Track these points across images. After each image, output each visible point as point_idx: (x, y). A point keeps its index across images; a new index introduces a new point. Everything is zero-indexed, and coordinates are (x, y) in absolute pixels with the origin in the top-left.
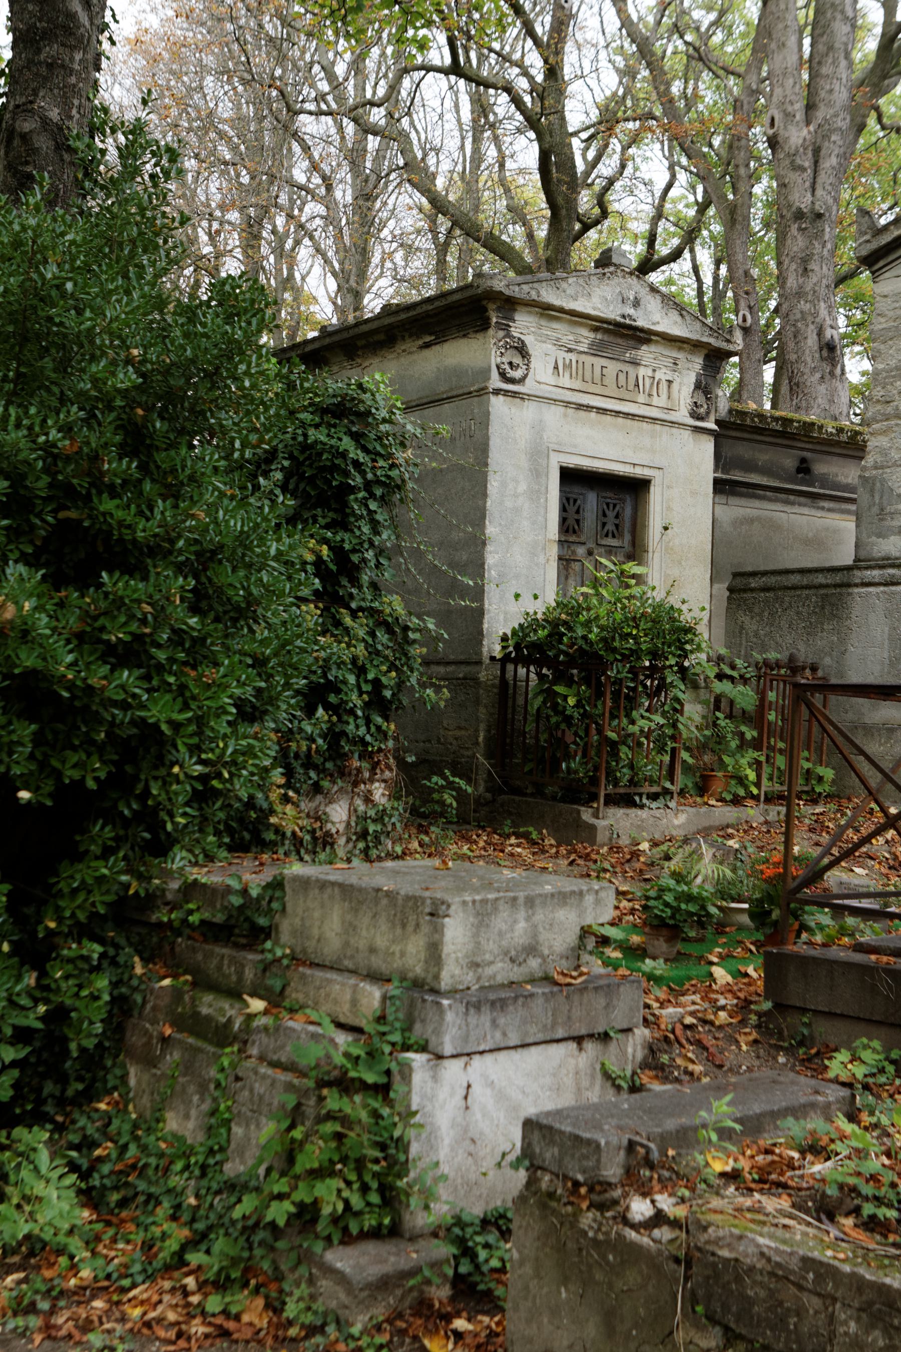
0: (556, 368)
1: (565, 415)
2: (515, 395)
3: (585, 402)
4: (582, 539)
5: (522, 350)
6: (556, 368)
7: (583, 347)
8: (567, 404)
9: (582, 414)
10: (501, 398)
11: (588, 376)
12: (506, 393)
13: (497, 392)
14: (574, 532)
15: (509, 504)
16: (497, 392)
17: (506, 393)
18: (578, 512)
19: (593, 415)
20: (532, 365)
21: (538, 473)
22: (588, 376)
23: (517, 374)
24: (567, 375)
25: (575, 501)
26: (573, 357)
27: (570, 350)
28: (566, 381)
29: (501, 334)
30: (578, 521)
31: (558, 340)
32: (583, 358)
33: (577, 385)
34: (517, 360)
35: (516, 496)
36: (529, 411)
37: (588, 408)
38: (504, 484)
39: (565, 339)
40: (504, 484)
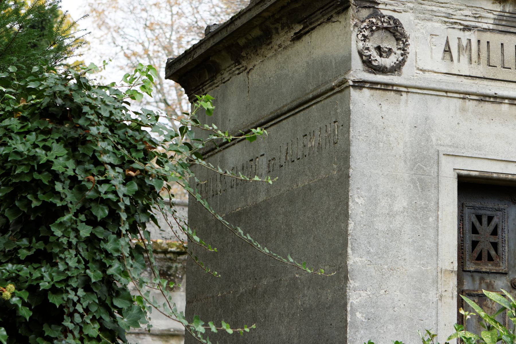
0: (448, 50)
1: (463, 110)
2: (386, 87)
3: (492, 92)
4: (503, 268)
5: (395, 31)
6: (448, 50)
7: (488, 23)
8: (465, 95)
9: (488, 107)
10: (366, 92)
11: (496, 58)
12: (373, 85)
13: (360, 85)
14: (490, 259)
15: (381, 226)
16: (360, 85)
17: (373, 85)
18: (495, 233)
19: (505, 107)
20: (411, 49)
21: (423, 183)
22: (496, 58)
23: (389, 62)
24: (464, 59)
25: (490, 219)
26: (473, 36)
27: (467, 28)
28: (463, 66)
29: (365, 13)
30: (495, 245)
31: (449, 16)
32: (487, 37)
33: (481, 70)
34: (389, 43)
35: (391, 215)
36: (409, 107)
37: (497, 99)
38: (373, 201)
39: (458, 15)
40: (373, 201)
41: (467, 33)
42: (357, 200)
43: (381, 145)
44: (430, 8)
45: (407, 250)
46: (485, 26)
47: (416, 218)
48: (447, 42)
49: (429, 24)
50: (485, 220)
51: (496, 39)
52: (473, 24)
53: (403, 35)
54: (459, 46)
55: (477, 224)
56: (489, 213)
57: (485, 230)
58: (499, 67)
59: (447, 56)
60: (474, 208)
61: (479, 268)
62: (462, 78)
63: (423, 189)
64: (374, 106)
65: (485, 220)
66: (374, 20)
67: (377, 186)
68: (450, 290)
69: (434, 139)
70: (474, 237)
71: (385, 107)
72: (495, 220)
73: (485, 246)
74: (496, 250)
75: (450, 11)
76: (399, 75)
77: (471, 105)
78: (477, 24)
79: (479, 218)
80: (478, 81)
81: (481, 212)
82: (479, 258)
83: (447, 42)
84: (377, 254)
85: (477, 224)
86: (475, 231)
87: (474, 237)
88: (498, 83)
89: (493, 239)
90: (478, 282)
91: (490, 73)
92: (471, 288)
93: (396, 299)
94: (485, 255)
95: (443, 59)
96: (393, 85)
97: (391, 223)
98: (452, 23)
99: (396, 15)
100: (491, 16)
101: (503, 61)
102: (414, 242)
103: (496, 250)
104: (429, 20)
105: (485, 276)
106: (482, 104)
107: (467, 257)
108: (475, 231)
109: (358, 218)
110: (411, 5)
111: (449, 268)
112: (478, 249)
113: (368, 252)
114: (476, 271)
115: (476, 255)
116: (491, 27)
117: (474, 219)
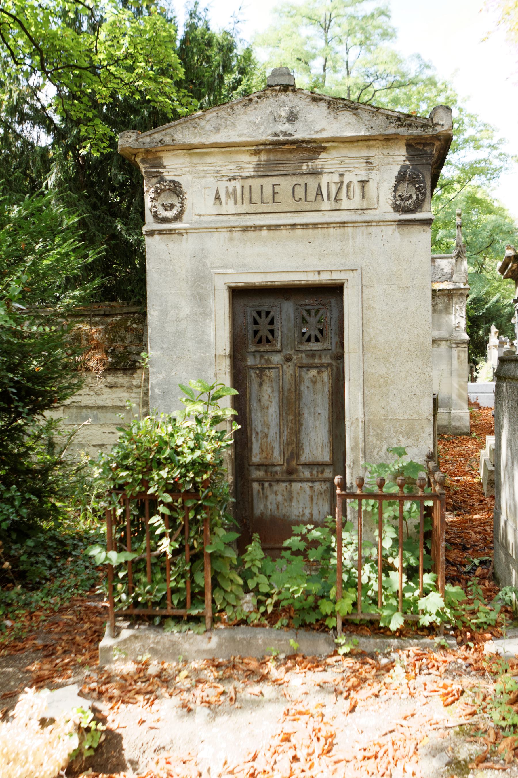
0: (218, 198)
1: (231, 239)
2: (170, 232)
3: (250, 224)
4: (278, 347)
5: (176, 189)
6: (218, 198)
7: (249, 171)
8: (231, 229)
9: (251, 234)
10: (157, 237)
11: (256, 197)
12: (161, 232)
13: (151, 233)
14: (268, 341)
15: (170, 328)
16: (151, 233)
17: (161, 232)
18: (272, 322)
19: (264, 232)
20: (186, 202)
21: (200, 297)
22: (256, 197)
23: (170, 214)
24: (231, 202)
25: (268, 313)
26: (237, 184)
27: (234, 178)
28: (230, 207)
29: (154, 180)
30: (272, 332)
31: (217, 172)
32: (250, 182)
33: (245, 208)
34: (174, 200)
35: (178, 320)
36: (189, 244)
37: (257, 228)
38: (164, 312)
39: (225, 170)
40: (164, 312)
41: (233, 182)
42: (152, 313)
43: (169, 273)
44: (202, 169)
45: (190, 343)
46: (248, 174)
47: (197, 321)
48: (217, 190)
49: (203, 181)
50: (263, 315)
51: (256, 183)
52: (238, 174)
53: (181, 193)
54: (227, 193)
55: (258, 318)
56: (267, 309)
57: (264, 321)
58: (259, 203)
59: (218, 202)
60: (253, 306)
61: (258, 349)
62: (230, 217)
63: (201, 300)
64: (163, 246)
65: (263, 315)
66: (158, 185)
67: (167, 302)
68: (223, 369)
69: (209, 264)
70: (255, 327)
71: (171, 245)
72: (272, 313)
73: (264, 332)
74: (273, 335)
75: (218, 168)
76: (181, 221)
77: (237, 235)
78: (241, 174)
79: (259, 313)
80: (242, 216)
81: (259, 309)
82: (260, 342)
83: (217, 190)
84: (168, 348)
85: (258, 318)
86: (256, 323)
87: (255, 327)
88: (259, 216)
89: (270, 327)
90: (258, 359)
91: (252, 209)
92: (253, 363)
93: (183, 378)
94: (264, 340)
95: (214, 204)
96: (175, 230)
97: (178, 326)
98: (221, 177)
99: (176, 179)
100: (251, 166)
101: (262, 198)
102: (195, 337)
103: (273, 335)
104: (204, 177)
105: (264, 354)
106: (246, 233)
107: (250, 342)
108: (256, 323)
109: (154, 325)
110: (188, 169)
111: (223, 353)
112: (259, 335)
113: (162, 348)
114: (256, 351)
115: (257, 340)
116: (252, 174)
117: (255, 314)
